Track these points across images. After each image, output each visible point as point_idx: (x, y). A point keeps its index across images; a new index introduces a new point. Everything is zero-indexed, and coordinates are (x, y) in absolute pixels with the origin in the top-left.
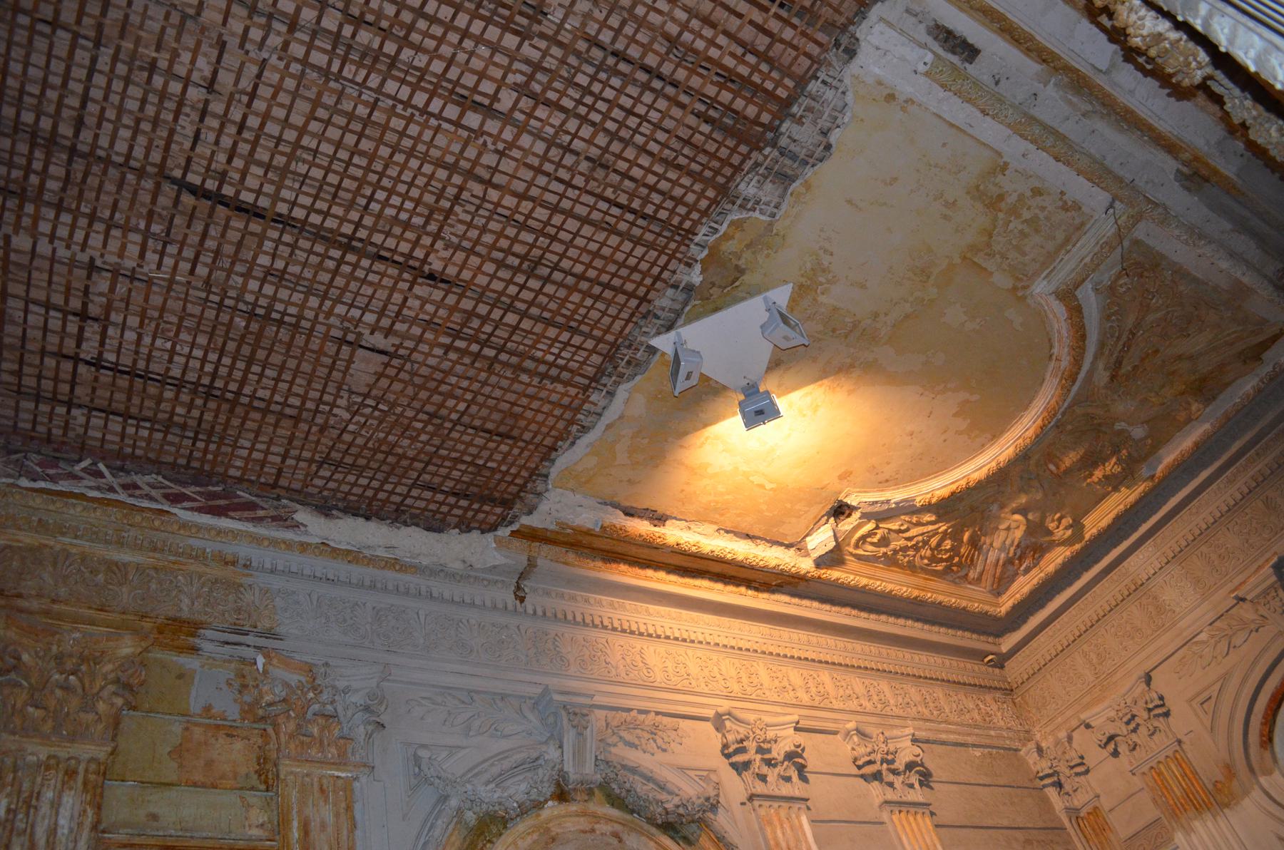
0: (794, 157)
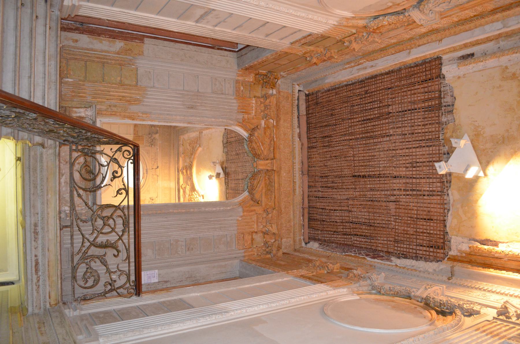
0: (449, 106)
